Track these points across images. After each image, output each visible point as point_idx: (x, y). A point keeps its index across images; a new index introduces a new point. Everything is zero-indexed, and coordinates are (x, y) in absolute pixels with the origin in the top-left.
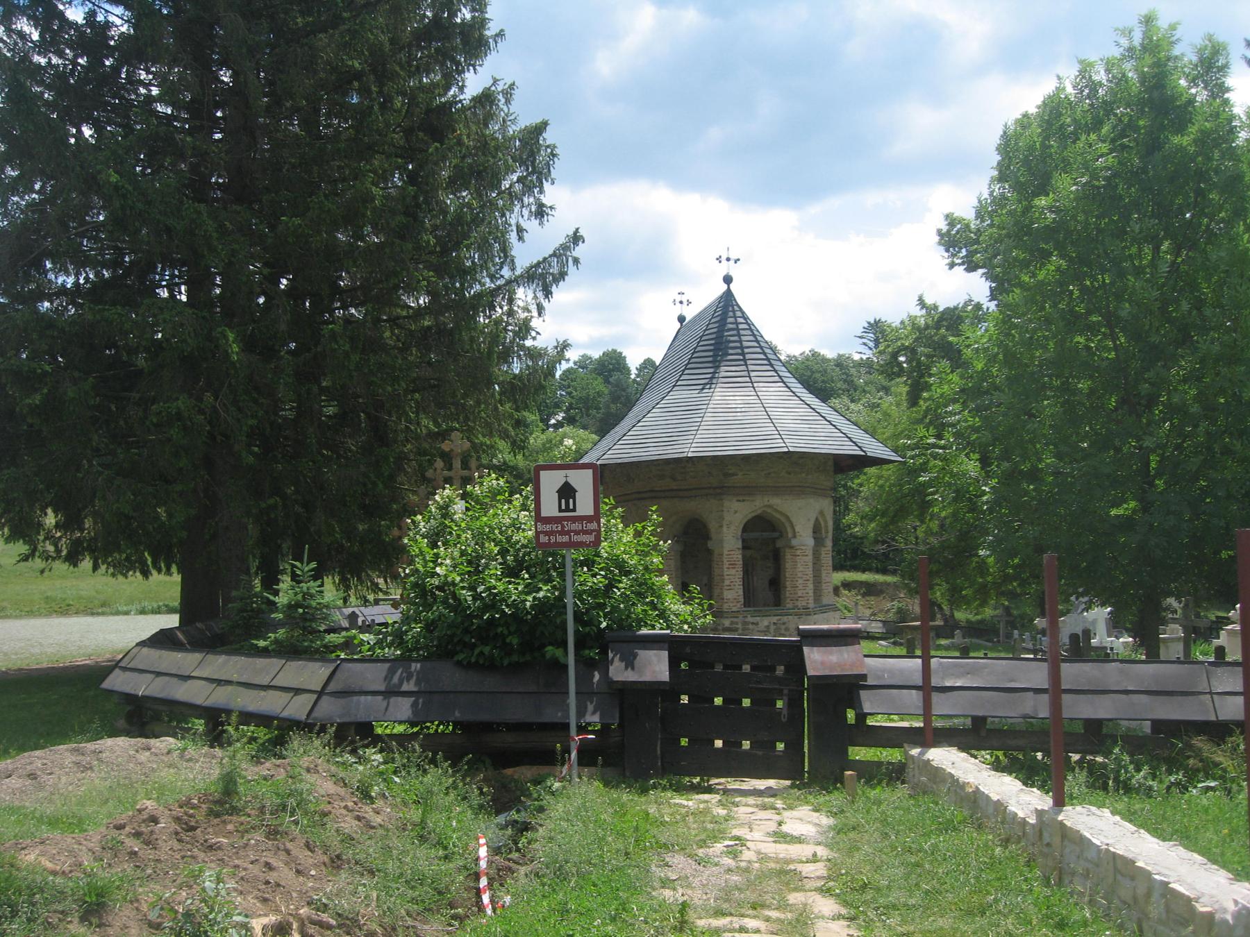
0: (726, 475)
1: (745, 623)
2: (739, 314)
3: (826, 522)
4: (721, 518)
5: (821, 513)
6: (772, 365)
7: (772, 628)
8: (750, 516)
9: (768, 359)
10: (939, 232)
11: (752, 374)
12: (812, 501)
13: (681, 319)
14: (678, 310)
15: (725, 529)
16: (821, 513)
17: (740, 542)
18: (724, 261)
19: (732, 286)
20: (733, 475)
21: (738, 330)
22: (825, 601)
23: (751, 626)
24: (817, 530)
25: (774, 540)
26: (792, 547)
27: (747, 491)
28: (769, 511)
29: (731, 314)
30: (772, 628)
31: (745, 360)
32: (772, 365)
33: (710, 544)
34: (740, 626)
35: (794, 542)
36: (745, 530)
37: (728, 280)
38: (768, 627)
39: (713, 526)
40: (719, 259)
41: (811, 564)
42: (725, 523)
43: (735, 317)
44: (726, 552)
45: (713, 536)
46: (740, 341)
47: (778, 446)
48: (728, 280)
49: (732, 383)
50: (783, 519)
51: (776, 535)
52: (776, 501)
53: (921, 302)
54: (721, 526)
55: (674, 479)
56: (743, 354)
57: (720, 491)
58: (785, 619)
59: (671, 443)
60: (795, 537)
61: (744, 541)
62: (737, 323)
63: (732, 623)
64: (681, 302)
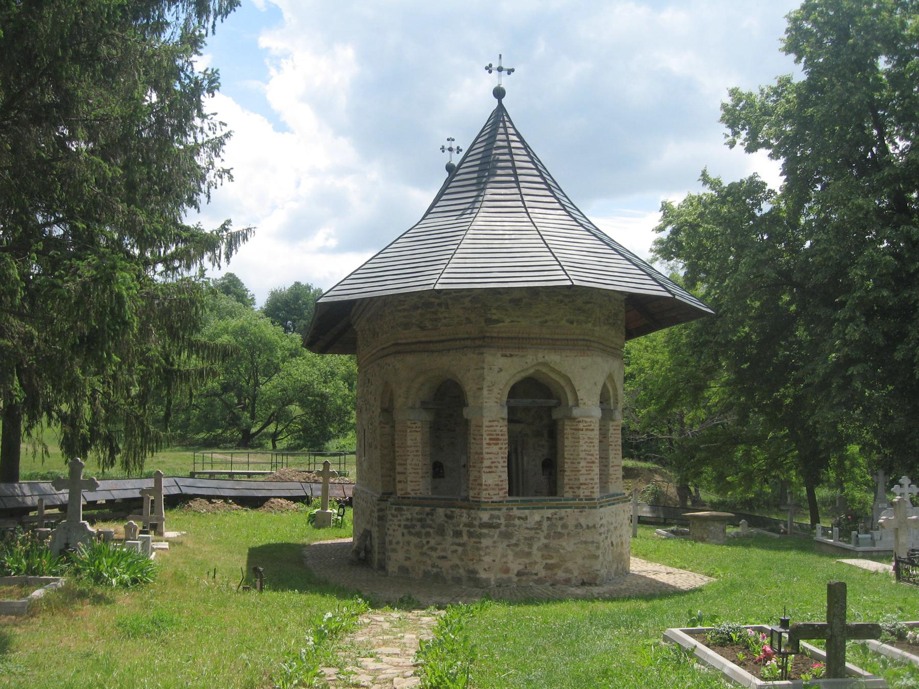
0: (489, 321)
1: (509, 518)
2: (511, 131)
3: (615, 389)
4: (482, 377)
5: (610, 377)
6: (552, 192)
7: (546, 524)
8: (518, 378)
9: (548, 185)
10: (724, 107)
11: (526, 198)
12: (599, 360)
13: (450, 168)
14: (446, 158)
15: (485, 392)
16: (610, 377)
17: (506, 411)
18: (495, 73)
19: (504, 101)
20: (498, 321)
21: (510, 147)
22: (613, 488)
23: (517, 522)
24: (604, 399)
25: (550, 409)
26: (574, 419)
27: (518, 343)
28: (544, 370)
29: (501, 130)
30: (546, 524)
31: (517, 182)
32: (552, 192)
33: (467, 413)
34: (502, 521)
35: (576, 412)
36: (514, 392)
37: (499, 93)
38: (539, 523)
39: (469, 388)
40: (489, 68)
41: (596, 442)
42: (485, 384)
43: (507, 134)
44: (486, 423)
45: (470, 401)
46: (513, 161)
47: (558, 279)
48: (499, 93)
49: (500, 208)
50: (562, 382)
51: (552, 402)
52: (554, 358)
53: (705, 178)
54: (481, 389)
55: (423, 328)
56: (515, 175)
57: (482, 342)
58: (563, 512)
59: (415, 275)
60: (577, 405)
61: (512, 410)
62: (509, 141)
63: (492, 517)
64: (450, 149)
